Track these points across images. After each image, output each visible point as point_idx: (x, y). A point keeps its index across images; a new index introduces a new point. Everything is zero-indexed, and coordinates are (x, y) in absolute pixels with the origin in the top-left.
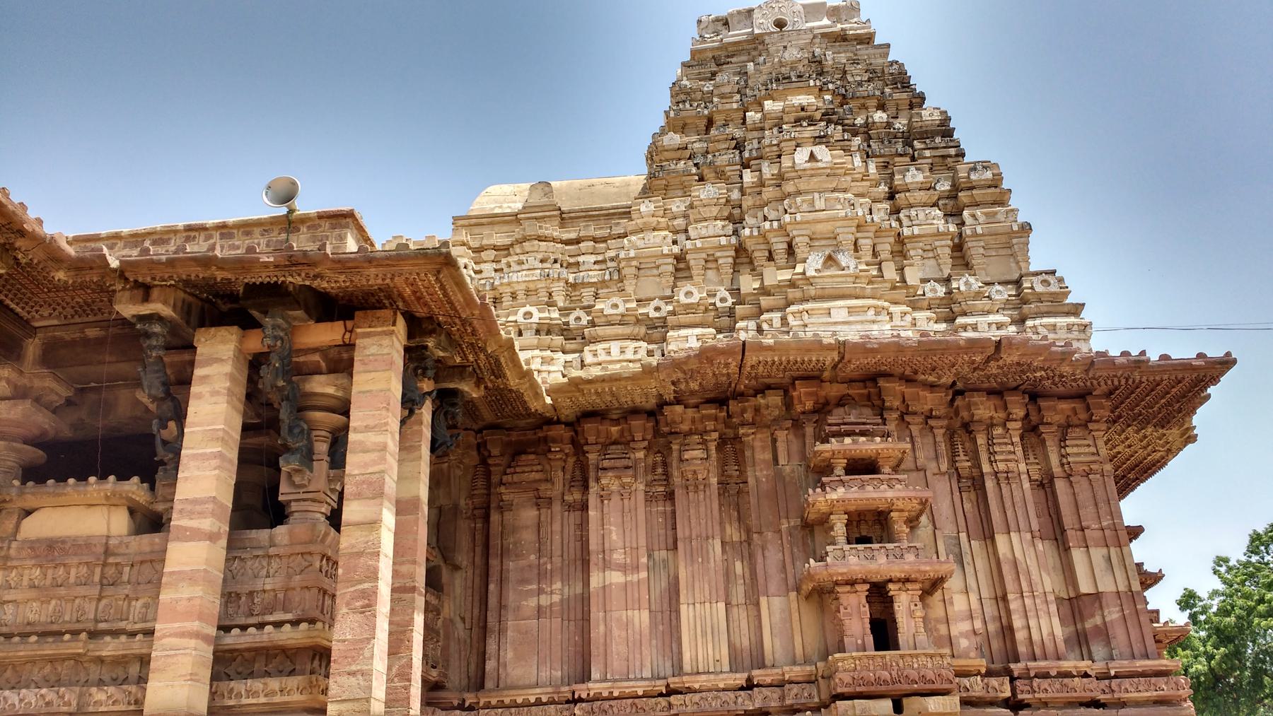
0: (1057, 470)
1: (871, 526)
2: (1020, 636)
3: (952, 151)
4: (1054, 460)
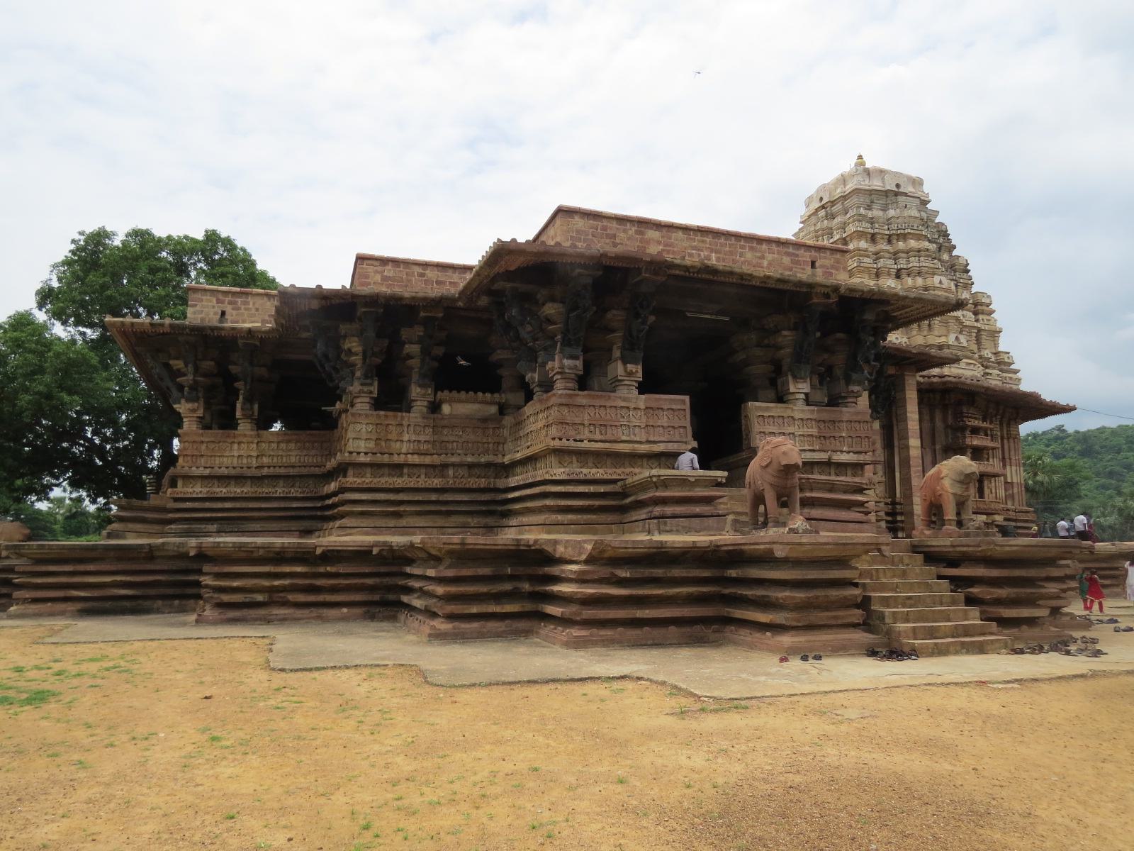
0: (1005, 436)
3: (970, 282)
4: (1005, 432)
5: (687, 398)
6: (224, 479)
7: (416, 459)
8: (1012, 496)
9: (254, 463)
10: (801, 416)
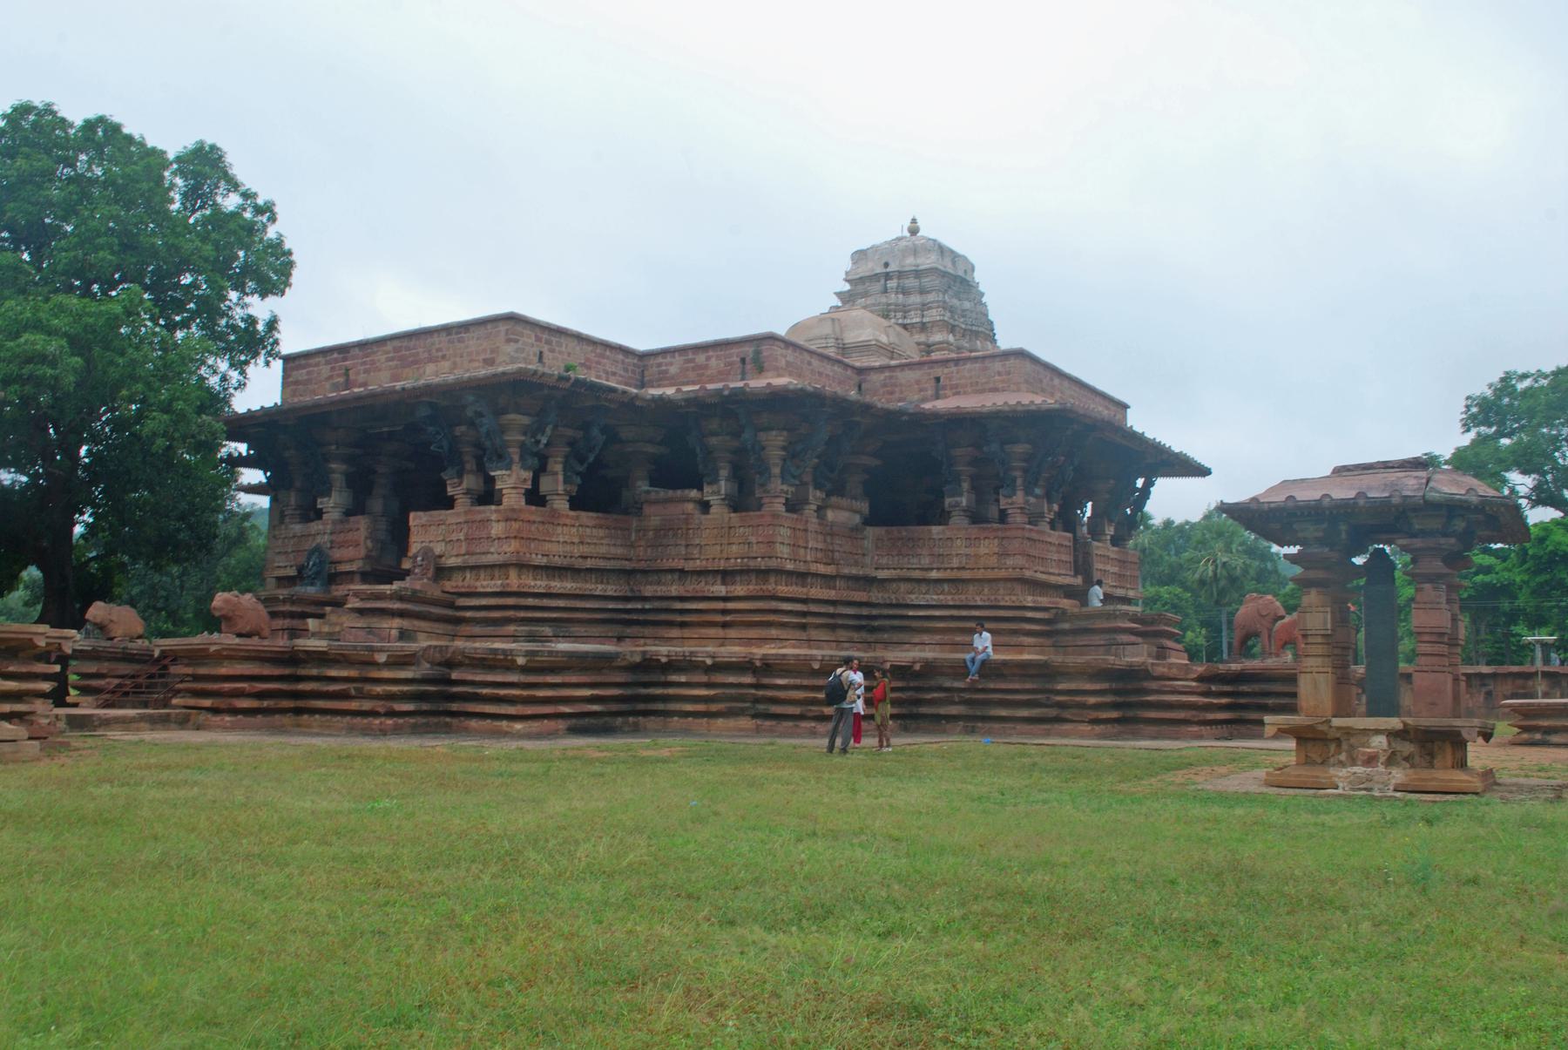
9: (577, 551)
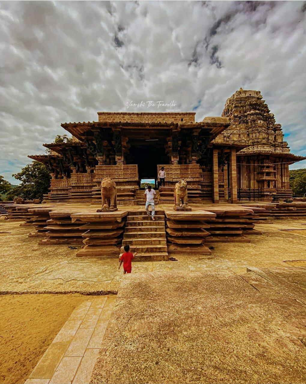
1: (268, 174)
2: (277, 186)
5: (137, 165)
6: (61, 190)
7: (86, 185)
8: (284, 186)
10: (175, 168)
